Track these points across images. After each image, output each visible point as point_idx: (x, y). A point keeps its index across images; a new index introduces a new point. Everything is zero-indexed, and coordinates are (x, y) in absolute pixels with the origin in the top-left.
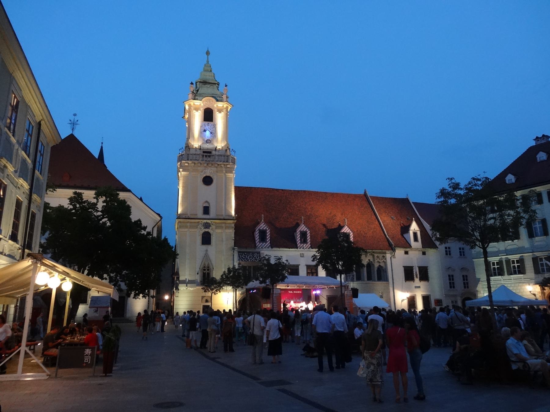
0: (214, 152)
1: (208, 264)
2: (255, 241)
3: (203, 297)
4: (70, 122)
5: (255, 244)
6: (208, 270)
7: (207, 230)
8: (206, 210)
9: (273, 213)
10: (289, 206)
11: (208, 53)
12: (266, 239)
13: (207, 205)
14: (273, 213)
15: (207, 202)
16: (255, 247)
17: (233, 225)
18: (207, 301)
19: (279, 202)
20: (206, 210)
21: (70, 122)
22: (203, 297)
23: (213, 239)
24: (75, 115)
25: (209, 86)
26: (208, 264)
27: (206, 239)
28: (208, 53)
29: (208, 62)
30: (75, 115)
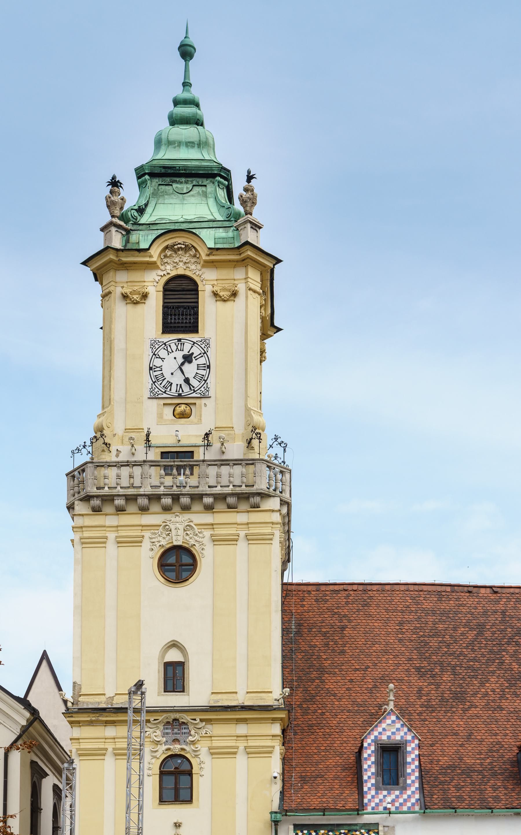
0: (199, 455)
5: (361, 794)
7: (176, 748)
8: (174, 676)
9: (447, 677)
10: (511, 649)
12: (405, 775)
13: (174, 656)
14: (447, 677)
15: (174, 645)
16: (360, 808)
17: (277, 729)
19: (471, 635)
20: (174, 676)
23: (202, 785)
27: (177, 782)
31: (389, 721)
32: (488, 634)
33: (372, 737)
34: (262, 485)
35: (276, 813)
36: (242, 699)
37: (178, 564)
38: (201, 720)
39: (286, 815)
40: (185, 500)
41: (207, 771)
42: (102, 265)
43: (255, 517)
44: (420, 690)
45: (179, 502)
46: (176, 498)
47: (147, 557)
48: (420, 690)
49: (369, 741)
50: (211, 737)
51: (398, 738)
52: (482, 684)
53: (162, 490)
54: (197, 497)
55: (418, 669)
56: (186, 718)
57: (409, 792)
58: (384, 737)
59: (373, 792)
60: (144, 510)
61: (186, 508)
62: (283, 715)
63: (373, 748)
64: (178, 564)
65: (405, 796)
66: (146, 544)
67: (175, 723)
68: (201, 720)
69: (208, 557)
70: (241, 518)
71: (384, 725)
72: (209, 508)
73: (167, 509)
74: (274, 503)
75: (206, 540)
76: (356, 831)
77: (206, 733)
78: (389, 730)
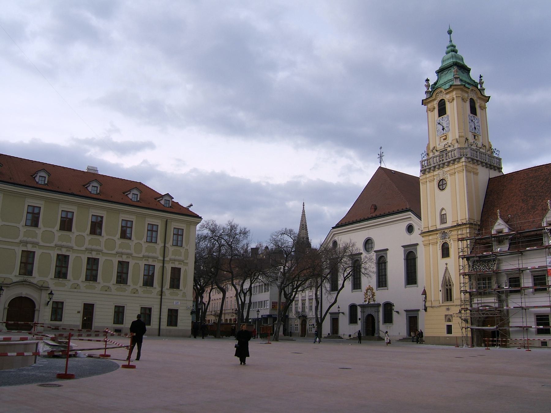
1: (449, 279)
3: (446, 316)
4: (378, 156)
6: (450, 285)
8: (443, 218)
11: (450, 32)
13: (443, 212)
15: (443, 209)
18: (449, 320)
20: (443, 218)
21: (378, 156)
22: (446, 316)
24: (381, 148)
25: (446, 72)
26: (449, 279)
28: (450, 32)
29: (451, 41)
30: (381, 148)
32: (549, 181)
34: (457, 156)
36: (460, 223)
37: (442, 185)
40: (441, 165)
41: (452, 247)
42: (424, 102)
43: (460, 165)
44: (522, 207)
45: (441, 166)
46: (439, 165)
47: (436, 183)
48: (522, 207)
52: (542, 201)
53: (436, 164)
54: (444, 164)
55: (523, 200)
56: (446, 231)
60: (434, 170)
61: (443, 167)
64: (442, 185)
66: (435, 181)
67: (444, 233)
69: (449, 180)
70: (456, 166)
72: (448, 166)
73: (439, 169)
74: (463, 159)
75: (448, 176)
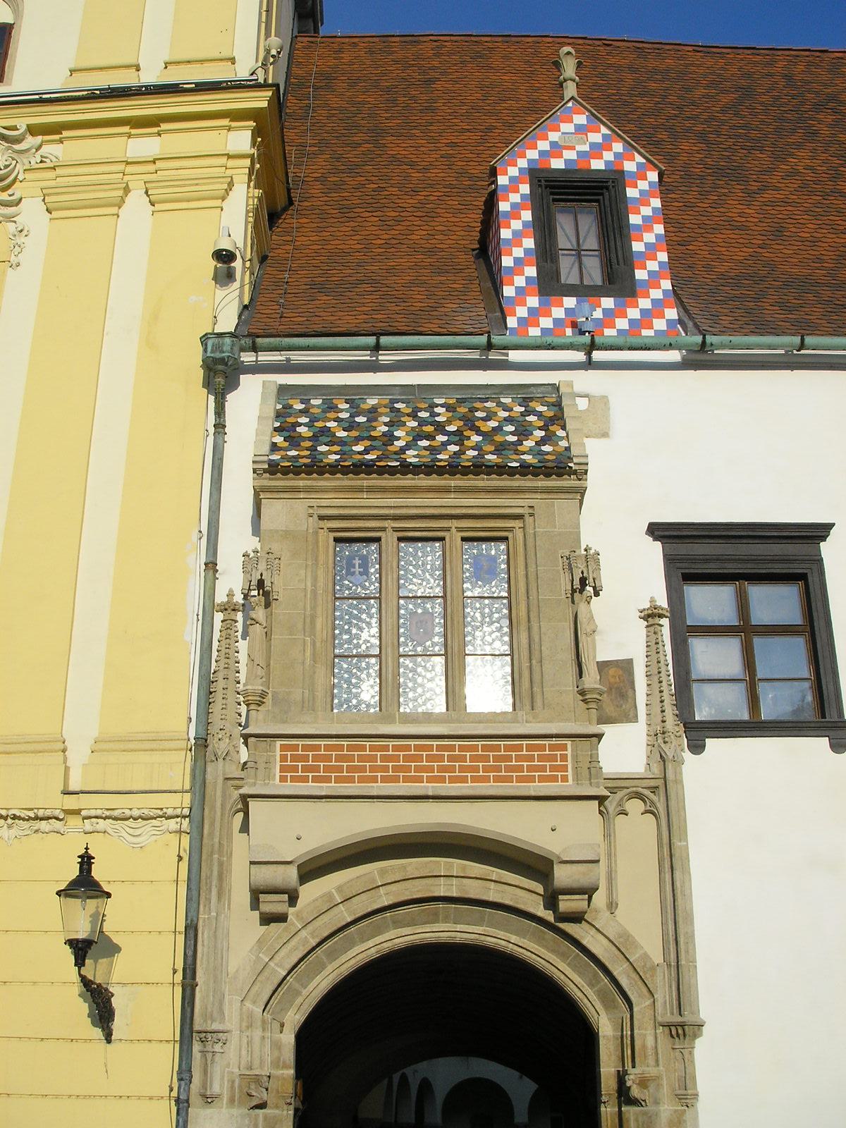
2: (494, 278)
17: (241, 140)
31: (567, 127)
33: (523, 163)
35: (220, 335)
38: (33, 130)
39: (255, 349)
49: (513, 172)
50: (54, 168)
51: (597, 165)
57: (645, 303)
58: (557, 164)
59: (533, 301)
62: (259, 100)
63: (525, 189)
65: (634, 313)
68: (33, 130)
71: (554, 136)
76: (487, 400)
77: (41, 162)
78: (573, 148)
